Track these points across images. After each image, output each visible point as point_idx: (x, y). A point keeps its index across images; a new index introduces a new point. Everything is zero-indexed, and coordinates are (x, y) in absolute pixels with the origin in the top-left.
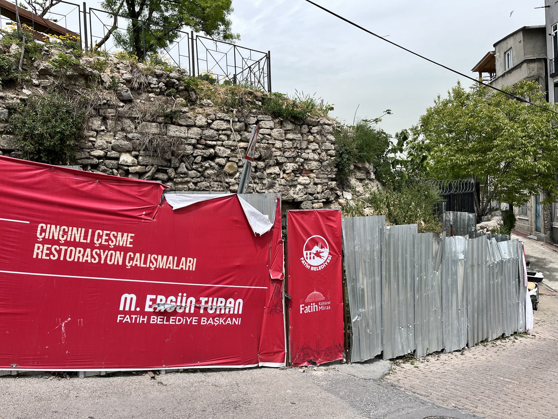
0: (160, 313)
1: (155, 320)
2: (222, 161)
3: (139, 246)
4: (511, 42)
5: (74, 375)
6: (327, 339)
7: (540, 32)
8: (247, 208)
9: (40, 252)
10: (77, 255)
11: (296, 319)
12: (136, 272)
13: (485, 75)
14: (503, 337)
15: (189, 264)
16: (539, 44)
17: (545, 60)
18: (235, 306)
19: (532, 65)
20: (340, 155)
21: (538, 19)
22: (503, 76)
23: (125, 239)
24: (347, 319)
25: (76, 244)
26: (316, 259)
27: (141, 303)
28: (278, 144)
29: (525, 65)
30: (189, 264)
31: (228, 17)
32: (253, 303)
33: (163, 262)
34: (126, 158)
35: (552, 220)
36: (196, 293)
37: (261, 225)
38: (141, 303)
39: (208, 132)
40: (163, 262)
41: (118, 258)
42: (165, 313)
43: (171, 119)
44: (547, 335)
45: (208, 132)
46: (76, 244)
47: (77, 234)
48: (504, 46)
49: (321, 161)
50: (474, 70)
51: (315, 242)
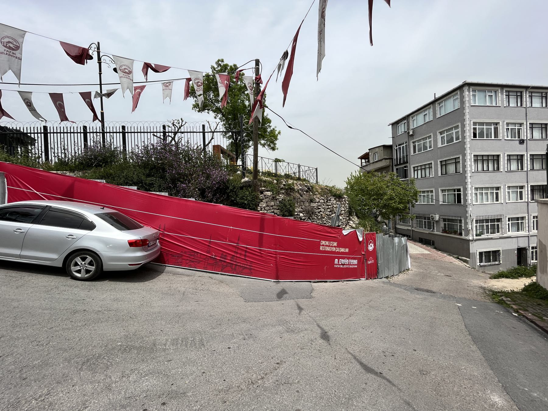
0: (342, 264)
1: (341, 266)
2: (322, 213)
3: (339, 246)
4: (377, 150)
5: (326, 282)
6: (373, 272)
7: (390, 147)
8: (358, 233)
9: (321, 248)
10: (328, 249)
11: (368, 265)
12: (338, 253)
13: (363, 161)
14: (404, 271)
15: (347, 250)
16: (389, 151)
17: (392, 159)
18: (355, 262)
19: (387, 161)
20: (350, 208)
21: (389, 142)
22: (373, 163)
23: (335, 244)
24: (377, 265)
25: (327, 246)
26: (371, 248)
27: (339, 262)
28: (335, 206)
29: (384, 160)
30: (347, 250)
31: (276, 142)
32: (359, 260)
33: (342, 250)
34: (301, 215)
35: (396, 224)
36: (348, 258)
37: (361, 239)
38: (339, 262)
39: (319, 204)
40: (342, 250)
41: (334, 249)
42: (343, 265)
43: (312, 201)
44: (416, 270)
45: (319, 204)
46: (327, 246)
47: (327, 243)
48: (374, 151)
49: (345, 211)
50: (359, 158)
51: (370, 242)
